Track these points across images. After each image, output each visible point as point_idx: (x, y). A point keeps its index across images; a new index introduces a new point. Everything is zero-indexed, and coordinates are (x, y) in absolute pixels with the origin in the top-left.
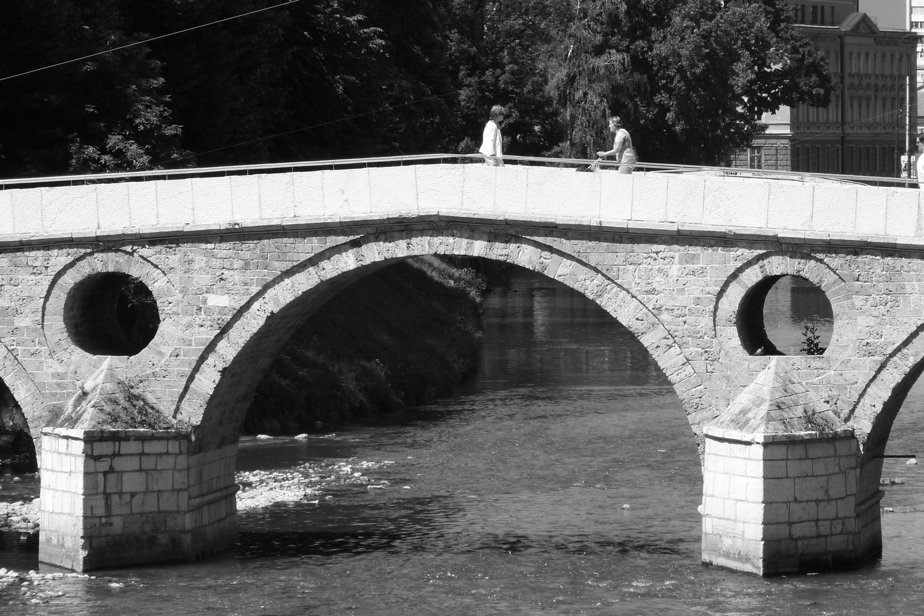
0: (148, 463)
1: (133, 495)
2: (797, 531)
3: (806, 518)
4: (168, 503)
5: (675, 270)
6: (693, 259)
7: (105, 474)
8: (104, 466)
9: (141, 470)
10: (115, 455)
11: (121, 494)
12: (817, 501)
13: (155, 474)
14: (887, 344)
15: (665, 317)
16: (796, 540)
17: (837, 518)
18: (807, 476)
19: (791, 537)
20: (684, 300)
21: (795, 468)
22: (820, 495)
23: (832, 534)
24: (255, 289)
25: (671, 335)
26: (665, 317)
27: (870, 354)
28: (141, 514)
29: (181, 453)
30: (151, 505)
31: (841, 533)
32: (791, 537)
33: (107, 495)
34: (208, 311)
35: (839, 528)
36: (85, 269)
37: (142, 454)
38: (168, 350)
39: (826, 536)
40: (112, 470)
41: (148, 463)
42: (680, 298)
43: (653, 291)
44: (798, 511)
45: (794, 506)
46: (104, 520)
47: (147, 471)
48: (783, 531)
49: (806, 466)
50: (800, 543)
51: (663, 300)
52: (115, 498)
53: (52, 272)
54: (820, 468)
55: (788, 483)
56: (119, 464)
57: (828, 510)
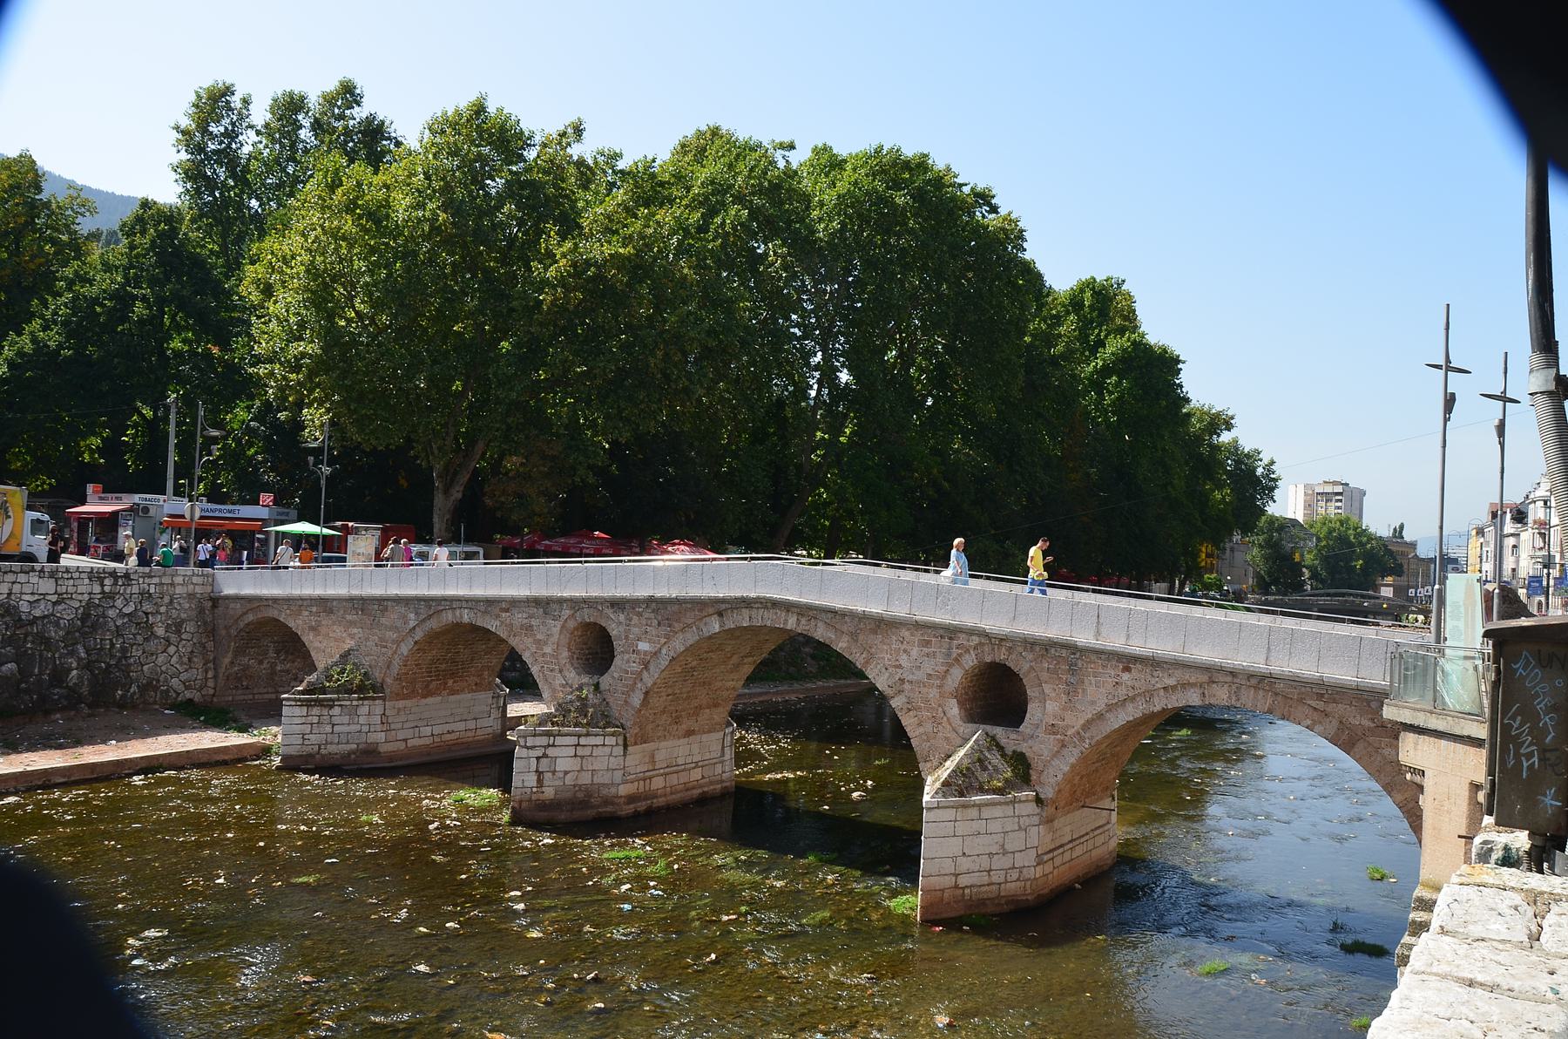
0: (580, 751)
1: (566, 773)
2: (964, 881)
3: (977, 869)
5: (915, 652)
6: (927, 643)
7: (538, 758)
8: (539, 753)
9: (576, 756)
11: (554, 772)
12: (990, 855)
13: (590, 759)
15: (907, 686)
16: (963, 888)
18: (979, 834)
19: (956, 887)
20: (920, 675)
23: (1006, 882)
27: (1054, 733)
28: (574, 786)
29: (617, 744)
30: (585, 779)
31: (1018, 880)
32: (956, 887)
35: (1015, 875)
38: (616, 675)
39: (1000, 884)
40: (545, 756)
41: (580, 751)
42: (917, 673)
43: (900, 666)
44: (965, 864)
46: (535, 790)
47: (582, 757)
50: (967, 891)
52: (548, 776)
56: (550, 751)
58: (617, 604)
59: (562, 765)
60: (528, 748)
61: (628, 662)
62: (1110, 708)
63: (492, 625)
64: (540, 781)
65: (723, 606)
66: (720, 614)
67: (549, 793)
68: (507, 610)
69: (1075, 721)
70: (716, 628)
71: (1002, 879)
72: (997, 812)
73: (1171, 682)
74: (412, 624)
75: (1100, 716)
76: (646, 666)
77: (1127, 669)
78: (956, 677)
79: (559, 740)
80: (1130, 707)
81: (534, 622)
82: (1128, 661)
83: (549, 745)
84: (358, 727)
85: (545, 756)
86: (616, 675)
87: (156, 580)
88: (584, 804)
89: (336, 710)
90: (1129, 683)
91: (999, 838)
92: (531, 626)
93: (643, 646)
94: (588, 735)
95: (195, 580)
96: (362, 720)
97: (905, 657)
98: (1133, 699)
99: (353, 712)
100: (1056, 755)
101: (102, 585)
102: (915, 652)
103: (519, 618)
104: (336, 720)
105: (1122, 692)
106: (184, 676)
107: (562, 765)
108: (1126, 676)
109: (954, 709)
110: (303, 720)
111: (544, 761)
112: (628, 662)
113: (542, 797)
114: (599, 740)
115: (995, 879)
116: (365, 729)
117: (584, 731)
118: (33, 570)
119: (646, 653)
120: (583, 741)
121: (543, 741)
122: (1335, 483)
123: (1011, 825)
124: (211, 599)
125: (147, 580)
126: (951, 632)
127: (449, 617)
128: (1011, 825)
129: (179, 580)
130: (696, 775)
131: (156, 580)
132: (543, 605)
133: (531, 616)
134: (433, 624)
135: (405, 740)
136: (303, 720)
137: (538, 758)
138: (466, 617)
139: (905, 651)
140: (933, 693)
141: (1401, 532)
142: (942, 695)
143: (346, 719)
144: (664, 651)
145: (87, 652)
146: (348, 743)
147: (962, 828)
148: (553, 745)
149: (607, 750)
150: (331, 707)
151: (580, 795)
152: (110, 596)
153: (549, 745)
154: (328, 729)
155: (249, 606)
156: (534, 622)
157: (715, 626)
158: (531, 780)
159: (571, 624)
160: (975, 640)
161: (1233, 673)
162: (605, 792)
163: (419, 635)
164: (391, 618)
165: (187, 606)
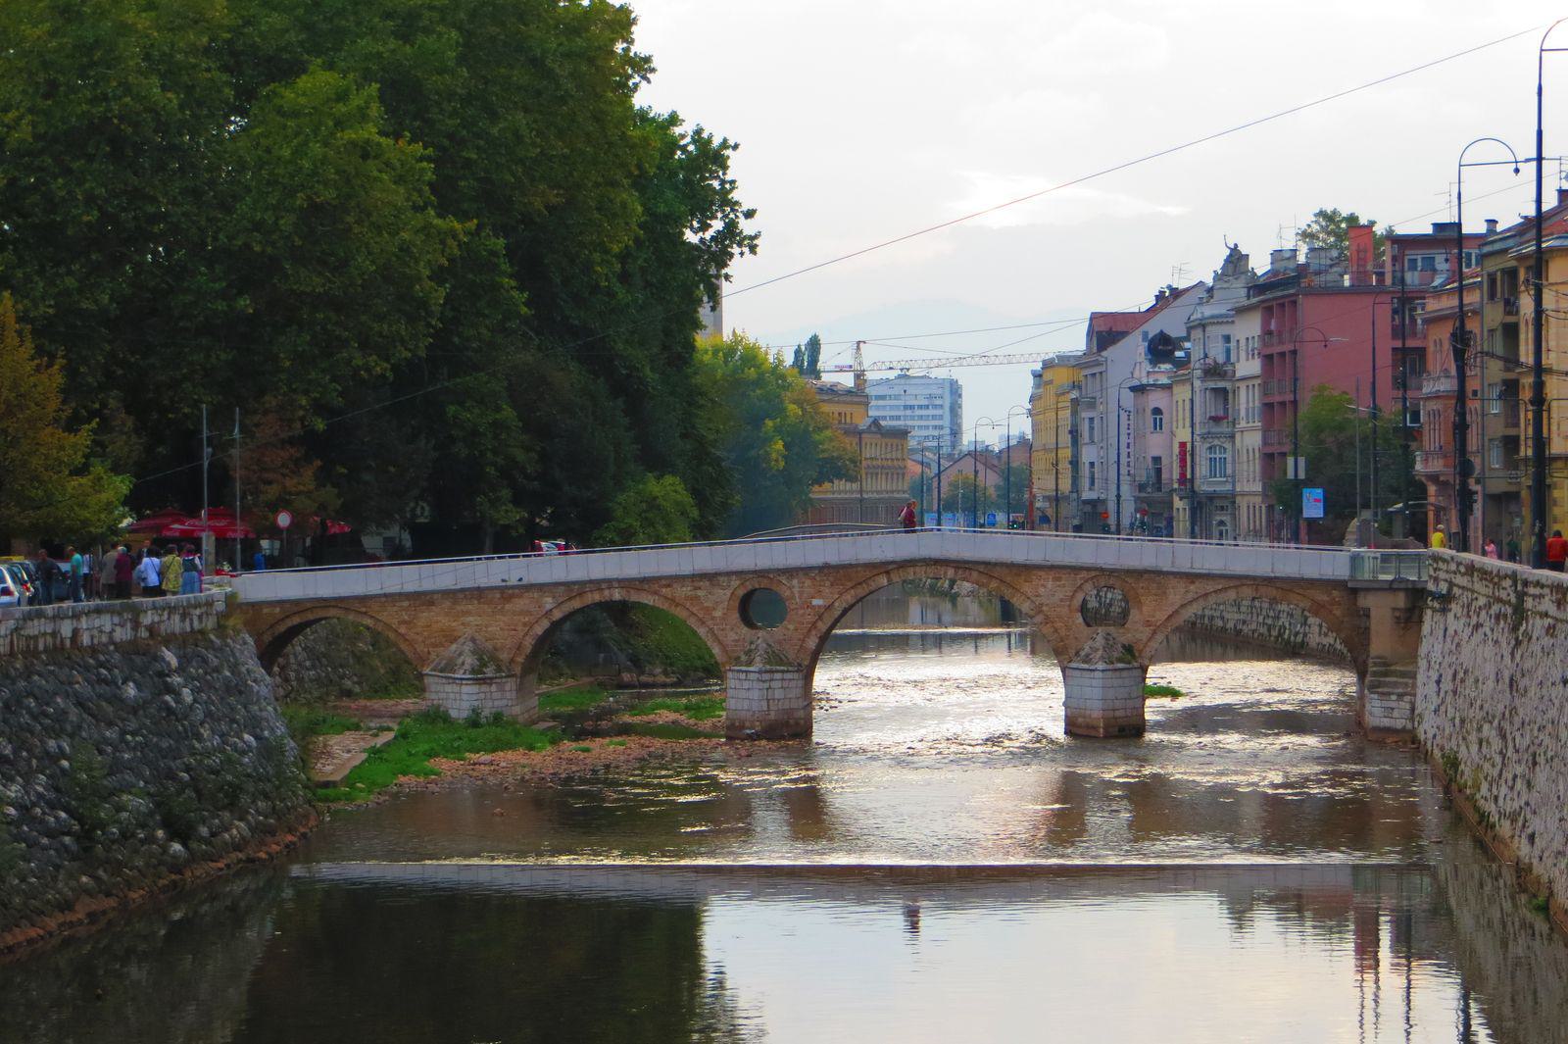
2: (1118, 714)
4: (794, 705)
5: (1050, 584)
6: (1059, 579)
8: (766, 685)
10: (771, 680)
21: (1116, 682)
22: (1126, 696)
25: (1047, 617)
26: (1044, 608)
33: (768, 700)
36: (749, 586)
37: (783, 679)
41: (786, 684)
44: (1118, 704)
48: (1111, 714)
49: (1120, 681)
51: (1044, 600)
61: (803, 615)
62: (1183, 606)
65: (891, 567)
66: (887, 572)
68: (669, 586)
69: (1161, 616)
72: (1125, 674)
74: (548, 607)
75: (1176, 612)
76: (820, 617)
77: (1193, 582)
81: (700, 593)
82: (1191, 577)
89: (494, 688)
92: (697, 598)
93: (816, 602)
94: (788, 671)
98: (1195, 600)
100: (1150, 640)
103: (682, 591)
104: (495, 695)
105: (1190, 596)
108: (1192, 587)
119: (819, 607)
132: (711, 577)
133: (696, 588)
134: (576, 604)
139: (1043, 585)
140: (1065, 611)
141: (814, 361)
142: (1071, 611)
144: (837, 604)
150: (491, 684)
155: (296, 609)
160: (1093, 574)
164: (520, 604)
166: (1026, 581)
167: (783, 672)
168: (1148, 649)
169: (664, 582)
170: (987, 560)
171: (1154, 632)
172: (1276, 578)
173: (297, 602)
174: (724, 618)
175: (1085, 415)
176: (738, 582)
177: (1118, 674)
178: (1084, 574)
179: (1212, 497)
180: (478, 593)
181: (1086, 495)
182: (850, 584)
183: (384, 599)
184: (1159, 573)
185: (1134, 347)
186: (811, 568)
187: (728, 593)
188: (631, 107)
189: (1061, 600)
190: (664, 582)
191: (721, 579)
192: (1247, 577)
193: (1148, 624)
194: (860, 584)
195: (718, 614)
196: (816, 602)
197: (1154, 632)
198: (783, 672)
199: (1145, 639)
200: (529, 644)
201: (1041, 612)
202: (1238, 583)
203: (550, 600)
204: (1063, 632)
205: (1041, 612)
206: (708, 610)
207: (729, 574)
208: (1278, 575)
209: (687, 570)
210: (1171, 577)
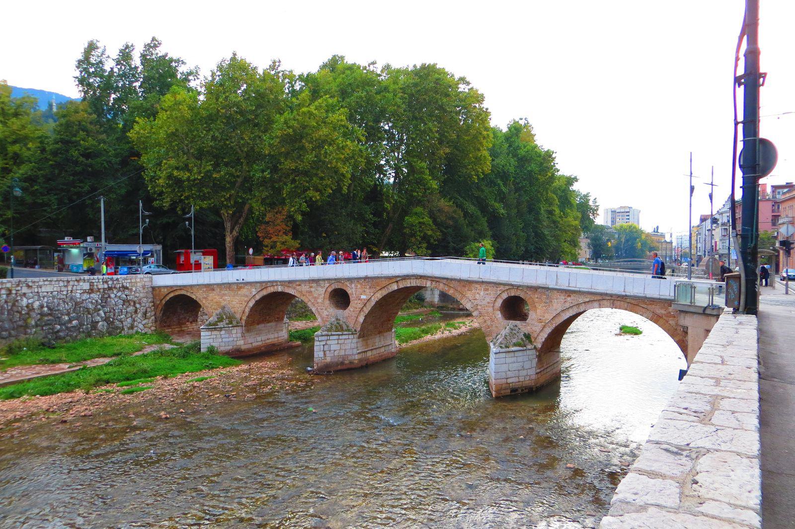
1: (335, 351)
2: (509, 381)
5: (482, 293)
6: (487, 290)
7: (323, 345)
8: (324, 343)
11: (330, 351)
14: (546, 319)
17: (527, 375)
19: (507, 383)
20: (484, 302)
24: (372, 294)
25: (480, 313)
26: (479, 307)
30: (342, 353)
34: (361, 300)
40: (326, 344)
41: (340, 342)
43: (476, 299)
44: (510, 374)
45: (509, 373)
50: (511, 385)
52: (328, 352)
53: (325, 288)
54: (520, 359)
55: (507, 365)
56: (329, 342)
57: (524, 373)
58: (351, 280)
59: (333, 347)
60: (320, 341)
61: (357, 304)
62: (563, 311)
63: (291, 291)
64: (325, 354)
65: (398, 279)
66: (397, 282)
67: (328, 360)
68: (300, 285)
69: (549, 317)
70: (396, 288)
71: (523, 380)
72: (520, 354)
73: (587, 300)
74: (254, 293)
77: (569, 296)
78: (499, 302)
79: (332, 337)
80: (571, 310)
81: (312, 290)
82: (568, 293)
83: (328, 340)
84: (231, 339)
85: (326, 344)
86: (352, 310)
87: (129, 281)
88: (342, 363)
89: (223, 332)
90: (570, 301)
91: (521, 364)
92: (311, 292)
93: (363, 297)
95: (145, 280)
96: (234, 336)
97: (478, 295)
99: (230, 333)
101: (108, 285)
102: (482, 293)
103: (305, 288)
105: (567, 305)
106: (144, 322)
107: (333, 347)
108: (569, 299)
109: (499, 315)
110: (210, 337)
111: (326, 348)
112: (357, 304)
113: (325, 361)
114: (346, 337)
115: (521, 380)
116: (235, 339)
117: (341, 333)
118: (80, 279)
119: (364, 299)
120: (341, 337)
121: (325, 338)
122: (624, 207)
123: (526, 358)
124: (152, 287)
125: (126, 281)
126: (497, 284)
127: (271, 290)
128: (526, 358)
129: (138, 280)
130: (382, 350)
131: (129, 281)
132: (316, 281)
133: (311, 287)
134: (265, 293)
135: (252, 343)
136: (210, 337)
137: (323, 345)
138: (280, 289)
139: (478, 293)
140: (490, 310)
141: (657, 230)
143: (227, 336)
144: (373, 298)
145: (105, 313)
146: (229, 346)
147: (509, 360)
148: (329, 340)
149: (350, 341)
150: (221, 331)
151: (341, 360)
152: (110, 289)
153: (328, 340)
154: (220, 340)
155: (171, 290)
156: (312, 290)
157: (395, 287)
158: (321, 354)
159: (330, 290)
160: (507, 287)
161: (611, 295)
162: (350, 358)
163: (258, 297)
164: (244, 291)
165: (142, 291)
166: (468, 290)
167: (339, 335)
168: (540, 337)
169: (298, 283)
170: (446, 277)
171: (544, 327)
172: (626, 296)
173: (171, 287)
174: (323, 303)
175: (699, 237)
176: (328, 285)
177: (512, 354)
178: (502, 287)
179: (722, 255)
180: (228, 286)
181: (698, 254)
182: (378, 288)
183: (198, 287)
184: (548, 289)
185: (709, 221)
186: (360, 278)
187: (324, 290)
188: (495, 132)
189: (488, 303)
190: (298, 283)
191: (321, 282)
192: (606, 294)
193: (540, 321)
194: (384, 287)
195: (320, 301)
196: (363, 297)
197: (544, 327)
198: (339, 335)
199: (538, 331)
200: (247, 310)
201: (477, 309)
202: (599, 298)
203: (254, 290)
204: (489, 323)
205: (477, 309)
206: (316, 298)
207: (324, 280)
208: (627, 294)
209: (307, 277)
210: (555, 292)
